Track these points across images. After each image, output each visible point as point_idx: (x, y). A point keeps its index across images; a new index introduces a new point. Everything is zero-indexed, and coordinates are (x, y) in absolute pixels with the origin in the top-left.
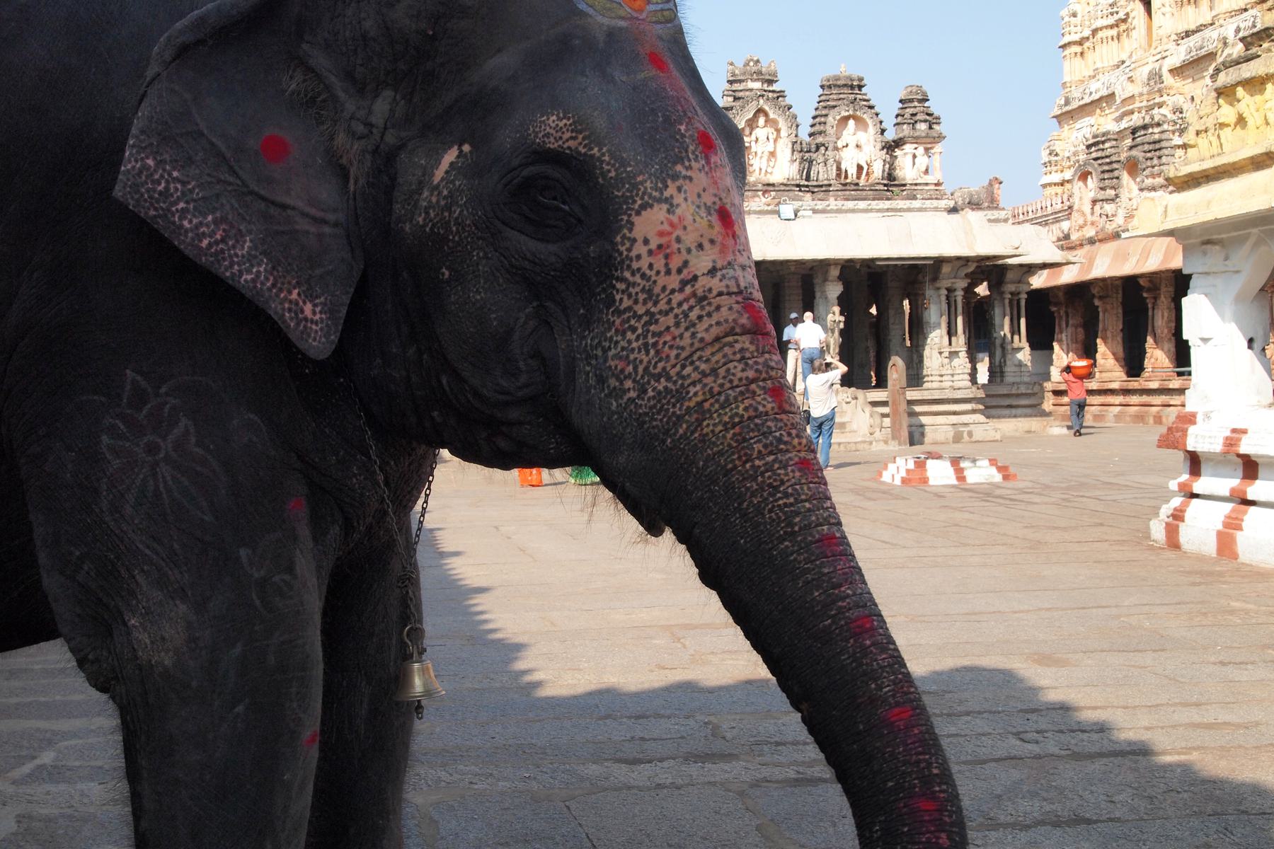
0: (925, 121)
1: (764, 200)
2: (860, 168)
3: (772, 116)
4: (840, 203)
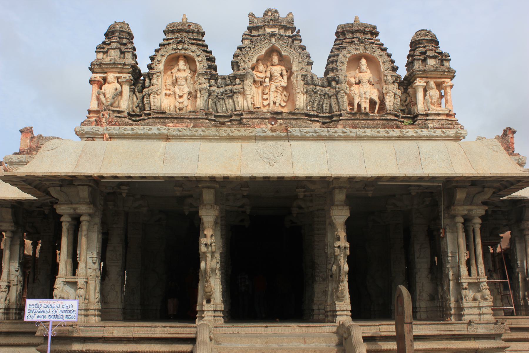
0: (434, 57)
1: (270, 126)
2: (372, 103)
3: (283, 53)
4: (348, 130)
